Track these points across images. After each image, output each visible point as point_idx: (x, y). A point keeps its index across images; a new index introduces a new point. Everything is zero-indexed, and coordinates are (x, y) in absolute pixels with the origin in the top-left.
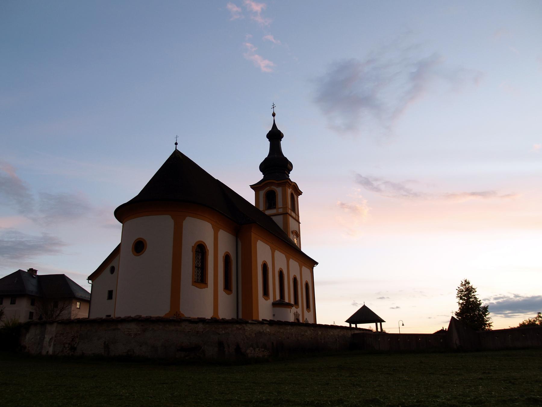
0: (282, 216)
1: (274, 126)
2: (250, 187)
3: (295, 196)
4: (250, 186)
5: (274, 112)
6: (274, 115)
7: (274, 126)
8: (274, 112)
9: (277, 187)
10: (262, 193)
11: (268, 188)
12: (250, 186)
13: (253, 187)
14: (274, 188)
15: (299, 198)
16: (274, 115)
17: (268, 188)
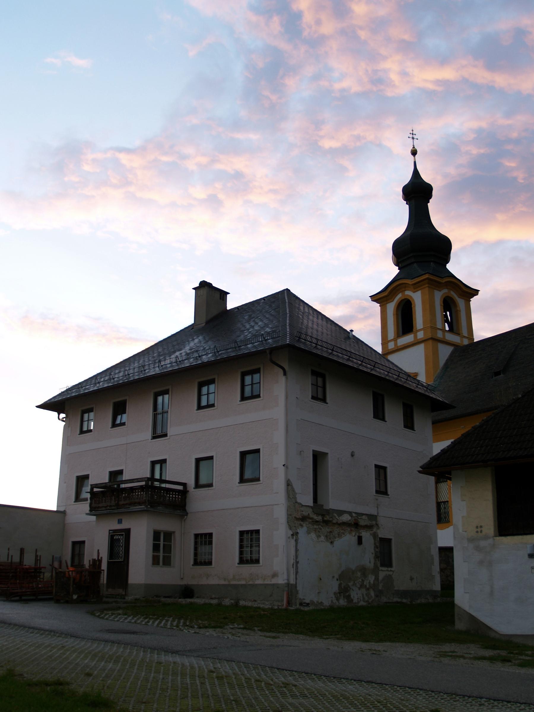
0: (422, 346)
1: (416, 173)
2: (370, 298)
3: (461, 302)
4: (370, 297)
5: (414, 147)
6: (414, 153)
7: (416, 173)
8: (414, 147)
9: (414, 292)
10: (391, 307)
11: (399, 297)
12: (370, 297)
13: (375, 298)
14: (408, 293)
15: (471, 302)
16: (414, 153)
17: (399, 297)
